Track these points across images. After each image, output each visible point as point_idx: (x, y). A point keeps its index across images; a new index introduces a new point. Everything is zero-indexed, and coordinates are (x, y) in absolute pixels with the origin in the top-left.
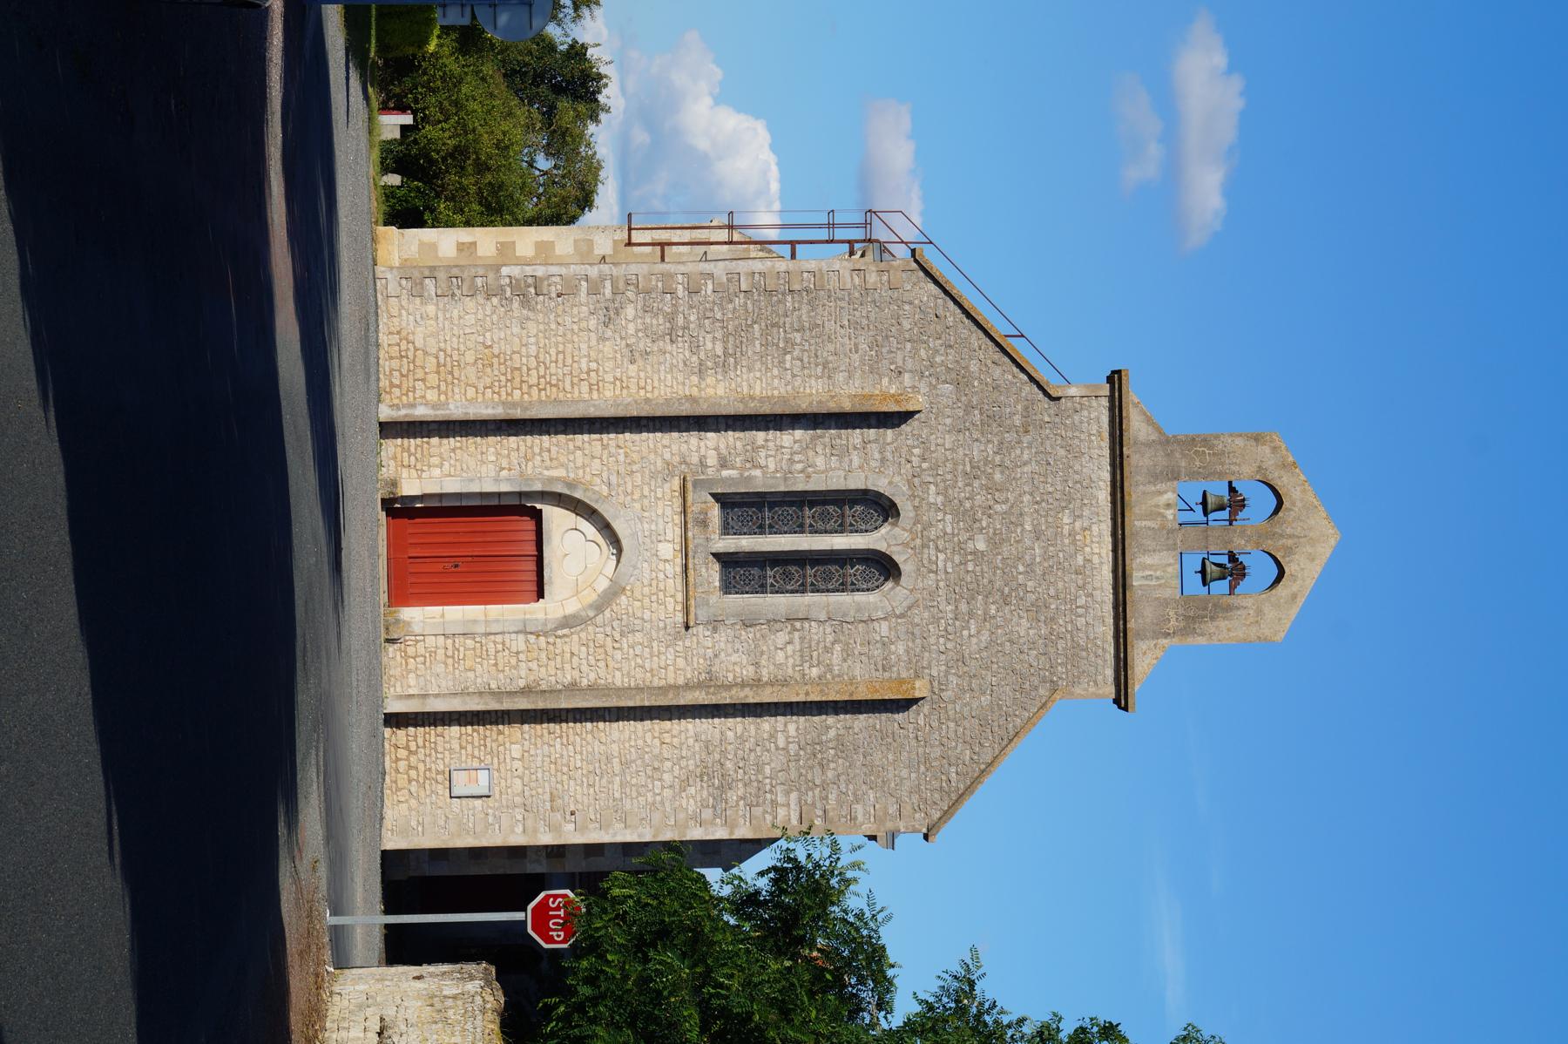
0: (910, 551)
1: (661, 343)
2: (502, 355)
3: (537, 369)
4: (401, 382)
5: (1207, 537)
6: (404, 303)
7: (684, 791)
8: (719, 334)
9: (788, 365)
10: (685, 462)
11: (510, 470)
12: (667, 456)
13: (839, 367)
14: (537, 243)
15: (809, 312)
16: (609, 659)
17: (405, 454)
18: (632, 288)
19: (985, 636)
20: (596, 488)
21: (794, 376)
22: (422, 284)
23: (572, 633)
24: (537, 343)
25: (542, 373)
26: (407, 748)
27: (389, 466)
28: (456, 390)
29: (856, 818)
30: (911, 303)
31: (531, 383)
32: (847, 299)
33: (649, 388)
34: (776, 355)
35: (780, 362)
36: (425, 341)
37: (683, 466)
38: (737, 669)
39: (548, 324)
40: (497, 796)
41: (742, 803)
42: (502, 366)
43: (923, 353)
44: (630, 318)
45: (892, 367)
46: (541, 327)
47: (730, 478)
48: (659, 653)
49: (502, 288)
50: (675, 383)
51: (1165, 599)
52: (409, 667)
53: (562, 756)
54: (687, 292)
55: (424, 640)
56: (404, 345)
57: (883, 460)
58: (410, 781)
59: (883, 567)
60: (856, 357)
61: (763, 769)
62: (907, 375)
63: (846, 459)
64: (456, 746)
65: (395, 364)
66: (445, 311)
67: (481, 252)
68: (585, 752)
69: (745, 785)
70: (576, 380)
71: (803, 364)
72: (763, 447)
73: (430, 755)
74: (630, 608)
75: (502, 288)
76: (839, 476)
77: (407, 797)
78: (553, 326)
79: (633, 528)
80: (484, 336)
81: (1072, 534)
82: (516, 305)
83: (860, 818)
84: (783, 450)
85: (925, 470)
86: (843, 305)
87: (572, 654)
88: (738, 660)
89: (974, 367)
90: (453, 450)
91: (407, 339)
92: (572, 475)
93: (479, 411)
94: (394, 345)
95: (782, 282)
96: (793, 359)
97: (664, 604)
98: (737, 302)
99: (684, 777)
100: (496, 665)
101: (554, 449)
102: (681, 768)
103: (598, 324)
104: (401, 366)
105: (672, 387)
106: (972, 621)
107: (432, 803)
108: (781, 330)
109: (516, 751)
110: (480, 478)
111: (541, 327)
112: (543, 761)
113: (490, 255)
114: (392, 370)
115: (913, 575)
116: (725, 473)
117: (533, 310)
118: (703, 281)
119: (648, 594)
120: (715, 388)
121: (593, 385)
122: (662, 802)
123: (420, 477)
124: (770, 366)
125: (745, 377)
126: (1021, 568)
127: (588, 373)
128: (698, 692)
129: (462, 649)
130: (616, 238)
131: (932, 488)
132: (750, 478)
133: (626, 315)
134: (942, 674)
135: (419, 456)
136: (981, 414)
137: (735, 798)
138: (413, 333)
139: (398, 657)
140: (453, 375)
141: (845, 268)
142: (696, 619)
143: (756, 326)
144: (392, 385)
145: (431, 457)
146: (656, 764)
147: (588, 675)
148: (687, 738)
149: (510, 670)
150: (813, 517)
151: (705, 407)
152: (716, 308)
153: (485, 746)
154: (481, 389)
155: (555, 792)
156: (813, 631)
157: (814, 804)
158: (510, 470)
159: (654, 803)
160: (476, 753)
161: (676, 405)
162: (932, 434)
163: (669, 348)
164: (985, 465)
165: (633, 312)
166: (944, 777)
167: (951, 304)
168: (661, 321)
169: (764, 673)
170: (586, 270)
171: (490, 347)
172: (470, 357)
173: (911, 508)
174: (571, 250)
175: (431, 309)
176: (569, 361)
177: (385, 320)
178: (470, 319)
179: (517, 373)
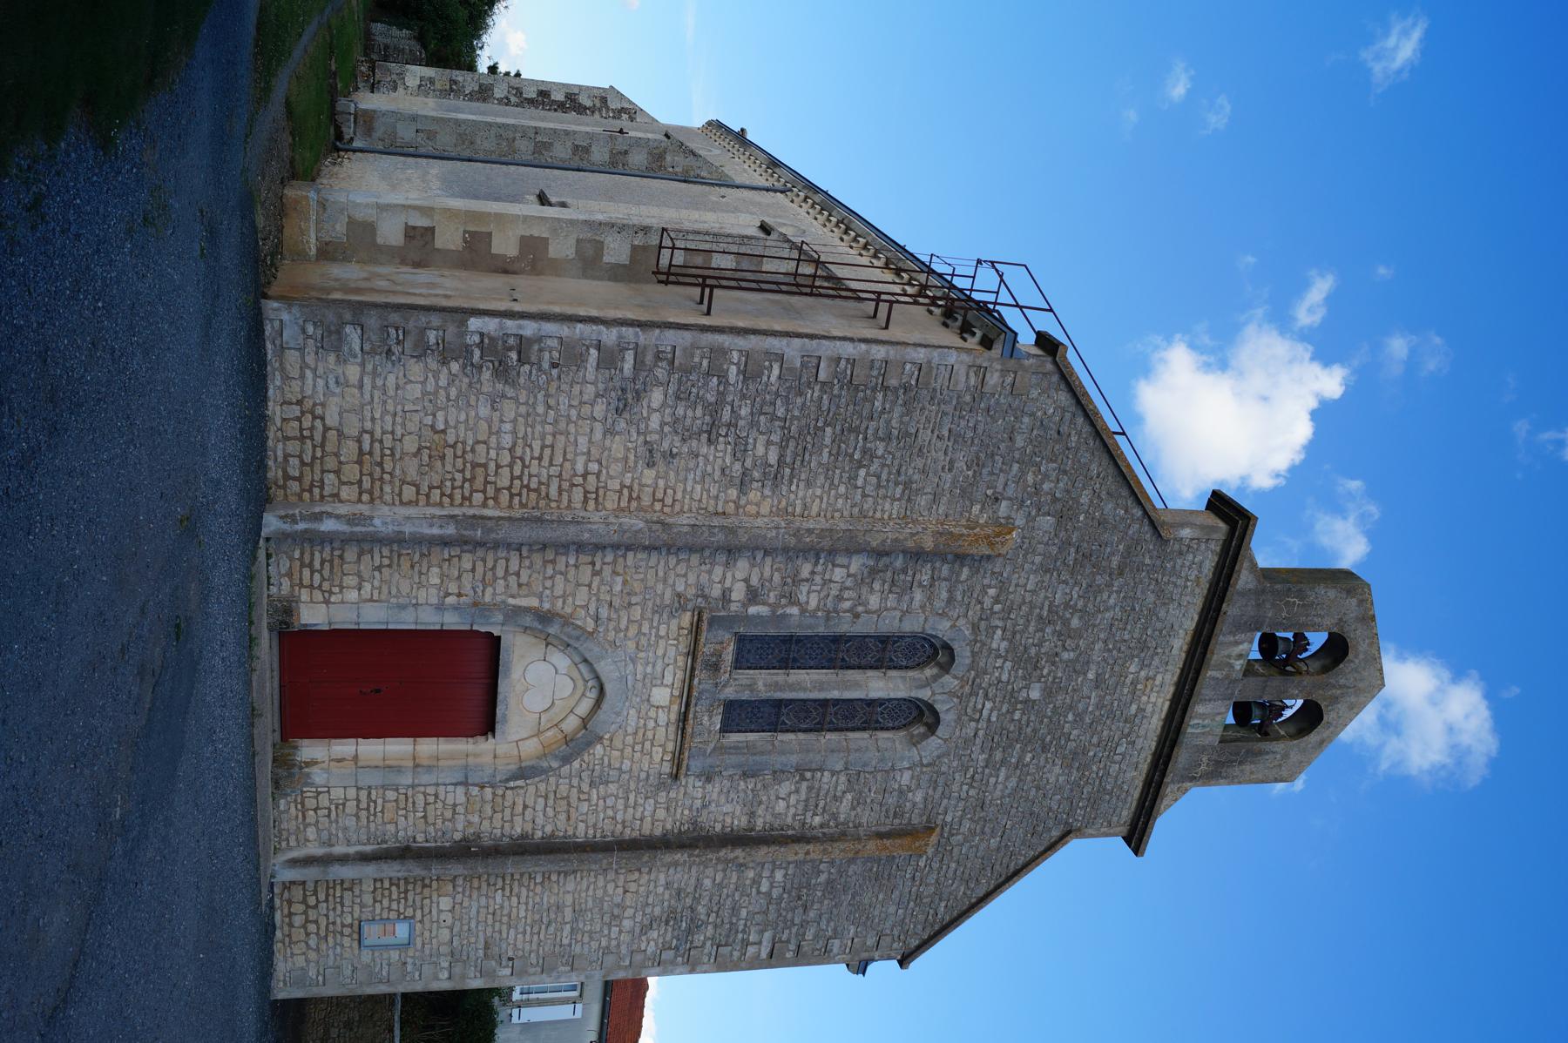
0: (955, 700)
1: (694, 443)
2: (460, 445)
3: (511, 466)
4: (301, 473)
5: (1264, 688)
6: (310, 359)
7: (646, 934)
8: (775, 438)
9: (860, 483)
10: (705, 597)
11: (459, 595)
12: (680, 588)
13: (924, 488)
14: (522, 237)
15: (901, 417)
16: (572, 810)
17: (306, 572)
18: (664, 364)
19: (1013, 783)
20: (579, 623)
21: (864, 496)
22: (339, 332)
23: (527, 785)
24: (514, 432)
25: (517, 472)
26: (304, 902)
27: (281, 584)
28: (387, 489)
29: (832, 950)
30: (1032, 415)
31: (500, 485)
32: (954, 402)
33: (669, 501)
34: (847, 469)
35: (850, 478)
36: (341, 418)
37: (700, 600)
38: (728, 820)
39: (534, 406)
40: (419, 945)
41: (709, 944)
42: (458, 460)
43: (1030, 478)
44: (655, 405)
45: (989, 492)
46: (523, 409)
47: (758, 616)
48: (635, 804)
49: (468, 350)
50: (705, 496)
51: (1203, 746)
52: (308, 821)
53: (502, 907)
54: (741, 377)
55: (328, 792)
56: (307, 423)
57: (950, 600)
58: (308, 934)
59: (921, 716)
60: (948, 477)
61: (739, 911)
62: (1004, 504)
63: (907, 598)
64: (368, 899)
65: (293, 447)
66: (375, 374)
67: (439, 243)
68: (531, 903)
69: (716, 927)
70: (565, 485)
71: (879, 482)
72: (807, 580)
73: (334, 909)
74: (606, 759)
75: (468, 350)
76: (894, 618)
77: (304, 950)
78: (541, 409)
79: (622, 669)
80: (434, 416)
81: (1134, 683)
82: (486, 375)
83: (835, 950)
84: (832, 585)
85: (995, 613)
86: (947, 410)
87: (525, 807)
88: (730, 810)
89: (1084, 500)
90: (379, 568)
91: (312, 412)
92: (547, 606)
93: (419, 530)
94: (292, 419)
95: (875, 373)
96: (868, 474)
97: (650, 754)
98: (809, 395)
99: (646, 922)
100: (425, 817)
101: (524, 575)
102: (644, 914)
103: (607, 410)
104: (302, 451)
105: (700, 501)
106: (1003, 769)
107: (335, 955)
108: (861, 436)
109: (445, 903)
110: (416, 605)
111: (523, 409)
112: (478, 912)
113: (453, 248)
114: (286, 456)
115: (953, 724)
116: (752, 610)
117: (514, 384)
118: (767, 363)
119: (631, 743)
120: (758, 505)
121: (589, 493)
122: (618, 945)
123: (327, 602)
124: (836, 482)
125: (801, 494)
126: (1070, 717)
127: (585, 476)
128: (679, 855)
129: (380, 801)
130: (636, 243)
131: (999, 632)
132: (784, 616)
133: (650, 401)
134: (956, 820)
135: (326, 573)
136: (1077, 552)
137: (702, 938)
138: (323, 405)
139: (293, 809)
140: (383, 469)
141: (962, 362)
142: (688, 769)
143: (829, 430)
144: (287, 477)
145: (345, 575)
146: (616, 911)
147: (543, 826)
148: (656, 887)
149: (443, 823)
150: (848, 651)
151: (744, 540)
152: (779, 402)
153: (406, 899)
154: (424, 489)
155: (490, 940)
156: (825, 780)
157: (788, 941)
158: (459, 595)
159: (608, 948)
160: (394, 906)
161: (706, 535)
162: (1014, 573)
163: (704, 450)
164: (1065, 609)
165: (661, 397)
166: (931, 912)
167: (1080, 420)
168: (699, 412)
169: (758, 823)
170: (600, 333)
171: (444, 432)
172: (410, 445)
173: (969, 654)
174: (570, 252)
175: (353, 372)
176: (559, 459)
177: (278, 383)
178: (415, 391)
179: (480, 471)
